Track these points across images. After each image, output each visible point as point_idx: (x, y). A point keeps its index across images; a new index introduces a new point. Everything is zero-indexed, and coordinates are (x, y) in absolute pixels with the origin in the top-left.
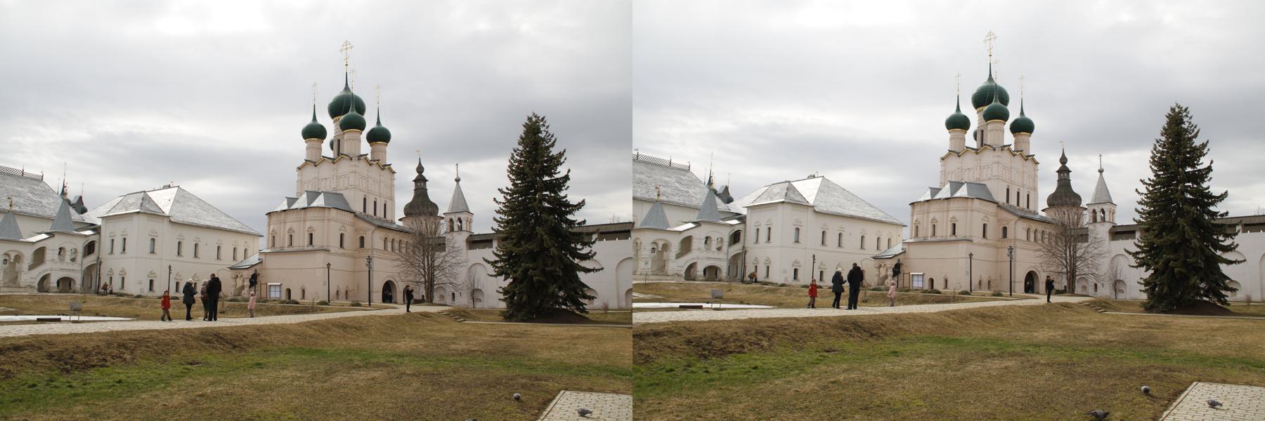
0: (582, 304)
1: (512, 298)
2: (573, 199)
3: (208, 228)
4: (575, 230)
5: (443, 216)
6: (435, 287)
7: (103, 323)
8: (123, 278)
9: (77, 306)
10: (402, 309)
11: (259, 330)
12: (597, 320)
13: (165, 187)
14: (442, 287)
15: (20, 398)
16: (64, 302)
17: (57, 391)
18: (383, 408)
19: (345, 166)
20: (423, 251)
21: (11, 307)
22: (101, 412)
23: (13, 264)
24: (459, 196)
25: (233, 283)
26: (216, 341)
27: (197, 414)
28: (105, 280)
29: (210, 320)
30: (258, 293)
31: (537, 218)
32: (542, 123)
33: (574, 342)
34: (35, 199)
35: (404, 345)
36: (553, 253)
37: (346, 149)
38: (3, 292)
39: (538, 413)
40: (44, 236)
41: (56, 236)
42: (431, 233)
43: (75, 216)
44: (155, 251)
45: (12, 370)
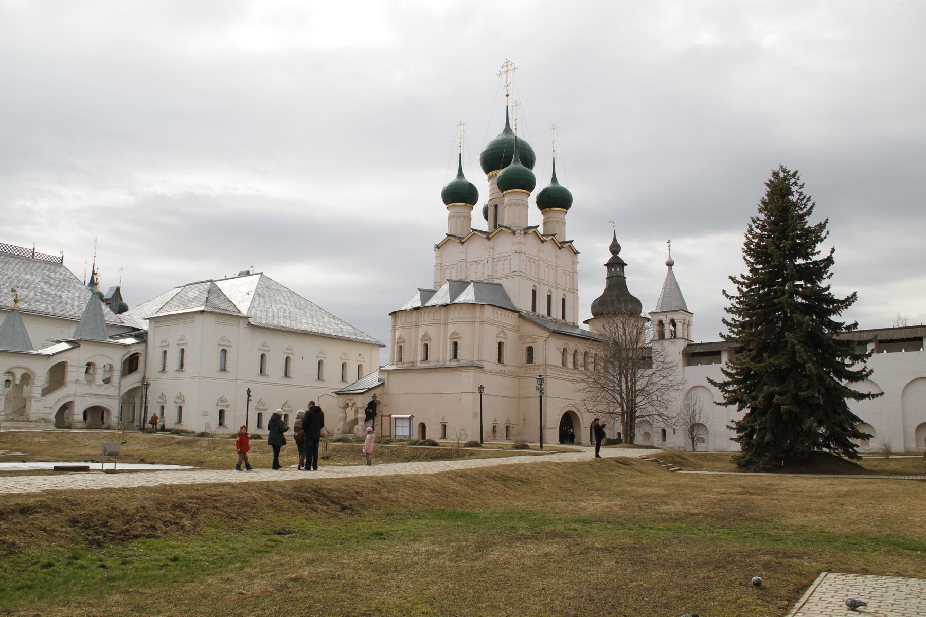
0: (853, 446)
1: (749, 436)
2: (839, 292)
3: (305, 334)
4: (842, 337)
5: (649, 316)
6: (637, 421)
7: (150, 474)
8: (180, 408)
9: (112, 449)
10: (588, 453)
11: (380, 483)
12: (874, 469)
13: (241, 275)
14: (647, 421)
15: (29, 583)
16: (93, 442)
17: (83, 573)
18: (560, 598)
19: (504, 244)
20: (620, 367)
21: (17, 450)
22: (147, 604)
23: (19, 387)
24: (672, 288)
25: (342, 415)
26: (316, 499)
27: (288, 607)
28: (153, 410)
29: (308, 469)
30: (377, 429)
31: (786, 320)
32: (793, 181)
33: (840, 501)
34: (51, 292)
35: (592, 505)
36: (810, 370)
37: (506, 218)
38: (5, 428)
39: (787, 606)
40: (65, 346)
41: (81, 346)
42: (631, 343)
43: (110, 316)
44: (228, 368)
45: (18, 542)
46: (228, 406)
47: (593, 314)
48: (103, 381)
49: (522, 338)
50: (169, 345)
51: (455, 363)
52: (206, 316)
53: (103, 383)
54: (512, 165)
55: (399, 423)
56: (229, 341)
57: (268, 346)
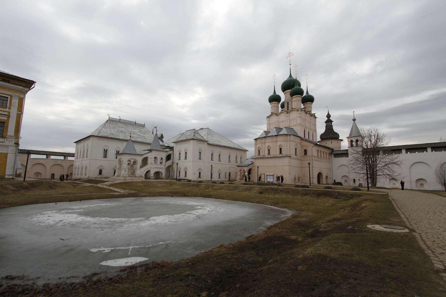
8: (186, 172)
23: (132, 166)
40: (147, 152)
44: (201, 158)
46: (202, 171)
47: (321, 139)
48: (160, 163)
49: (302, 146)
50: (181, 151)
51: (281, 155)
52: (194, 141)
53: (160, 164)
54: (295, 87)
55: (268, 177)
56: (202, 149)
57: (213, 151)
